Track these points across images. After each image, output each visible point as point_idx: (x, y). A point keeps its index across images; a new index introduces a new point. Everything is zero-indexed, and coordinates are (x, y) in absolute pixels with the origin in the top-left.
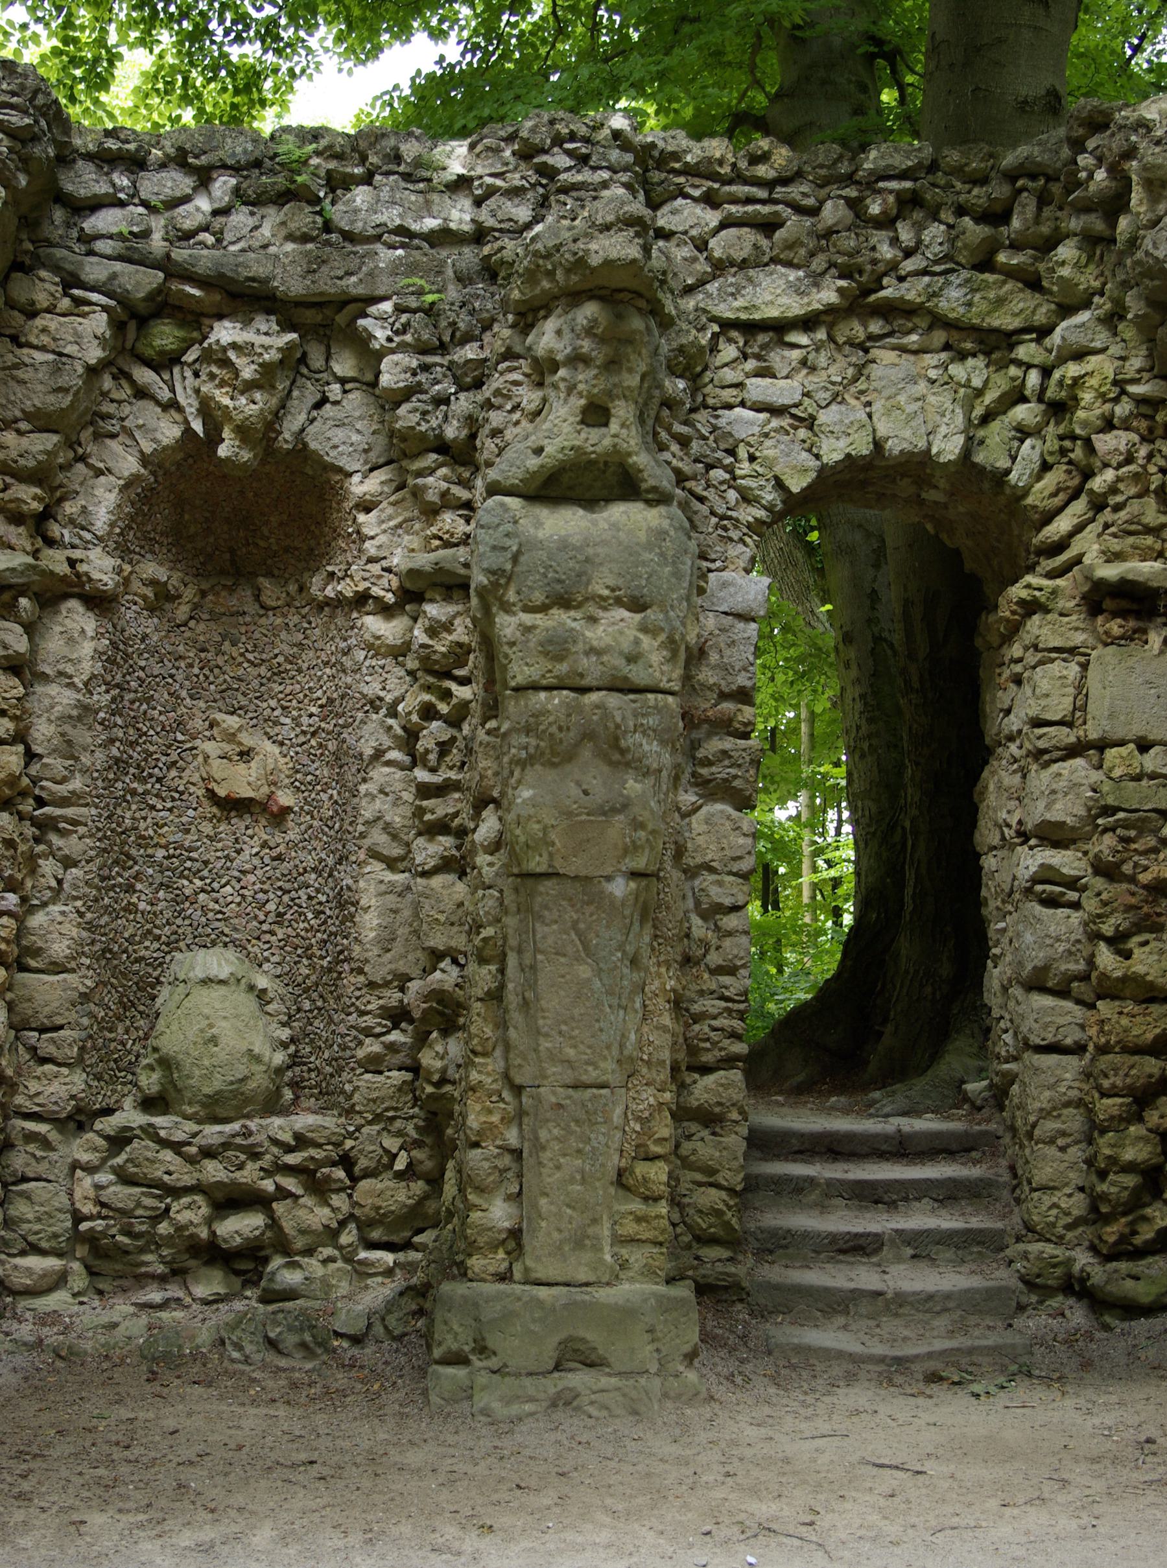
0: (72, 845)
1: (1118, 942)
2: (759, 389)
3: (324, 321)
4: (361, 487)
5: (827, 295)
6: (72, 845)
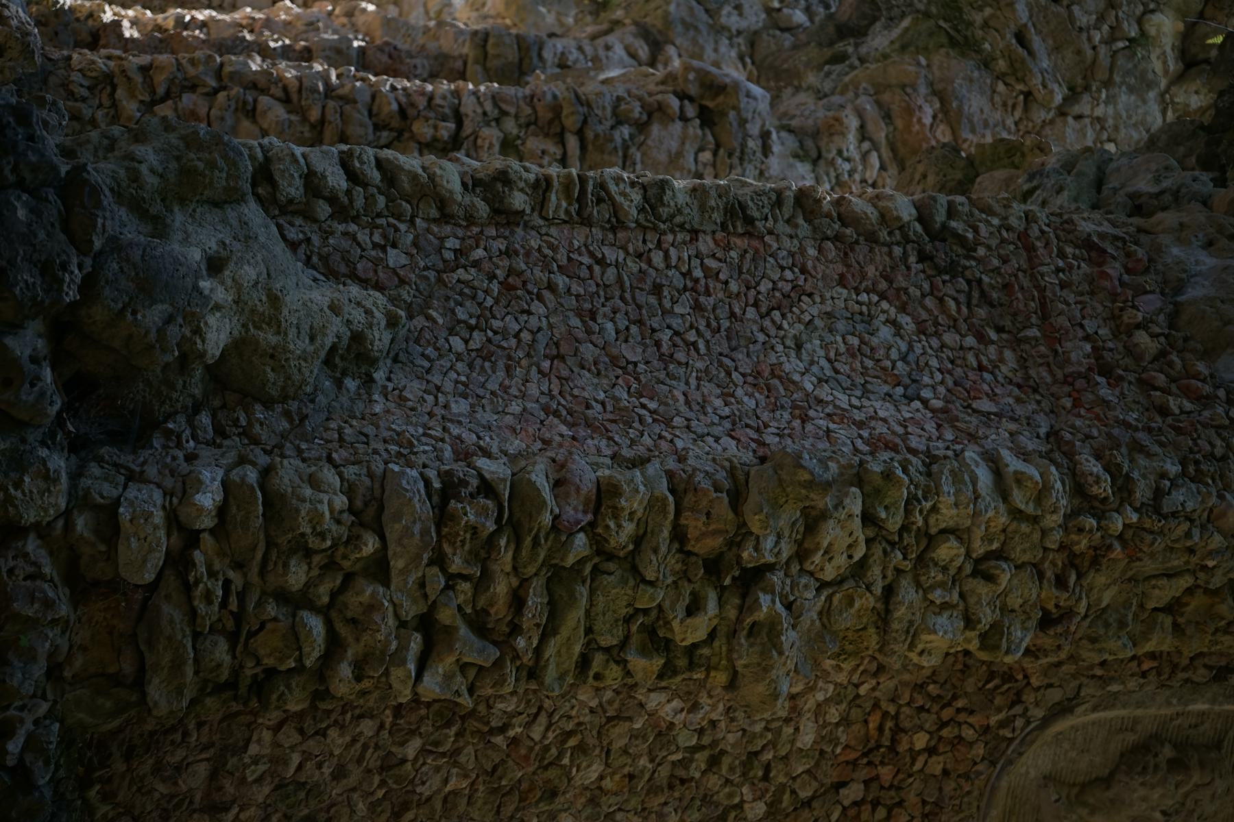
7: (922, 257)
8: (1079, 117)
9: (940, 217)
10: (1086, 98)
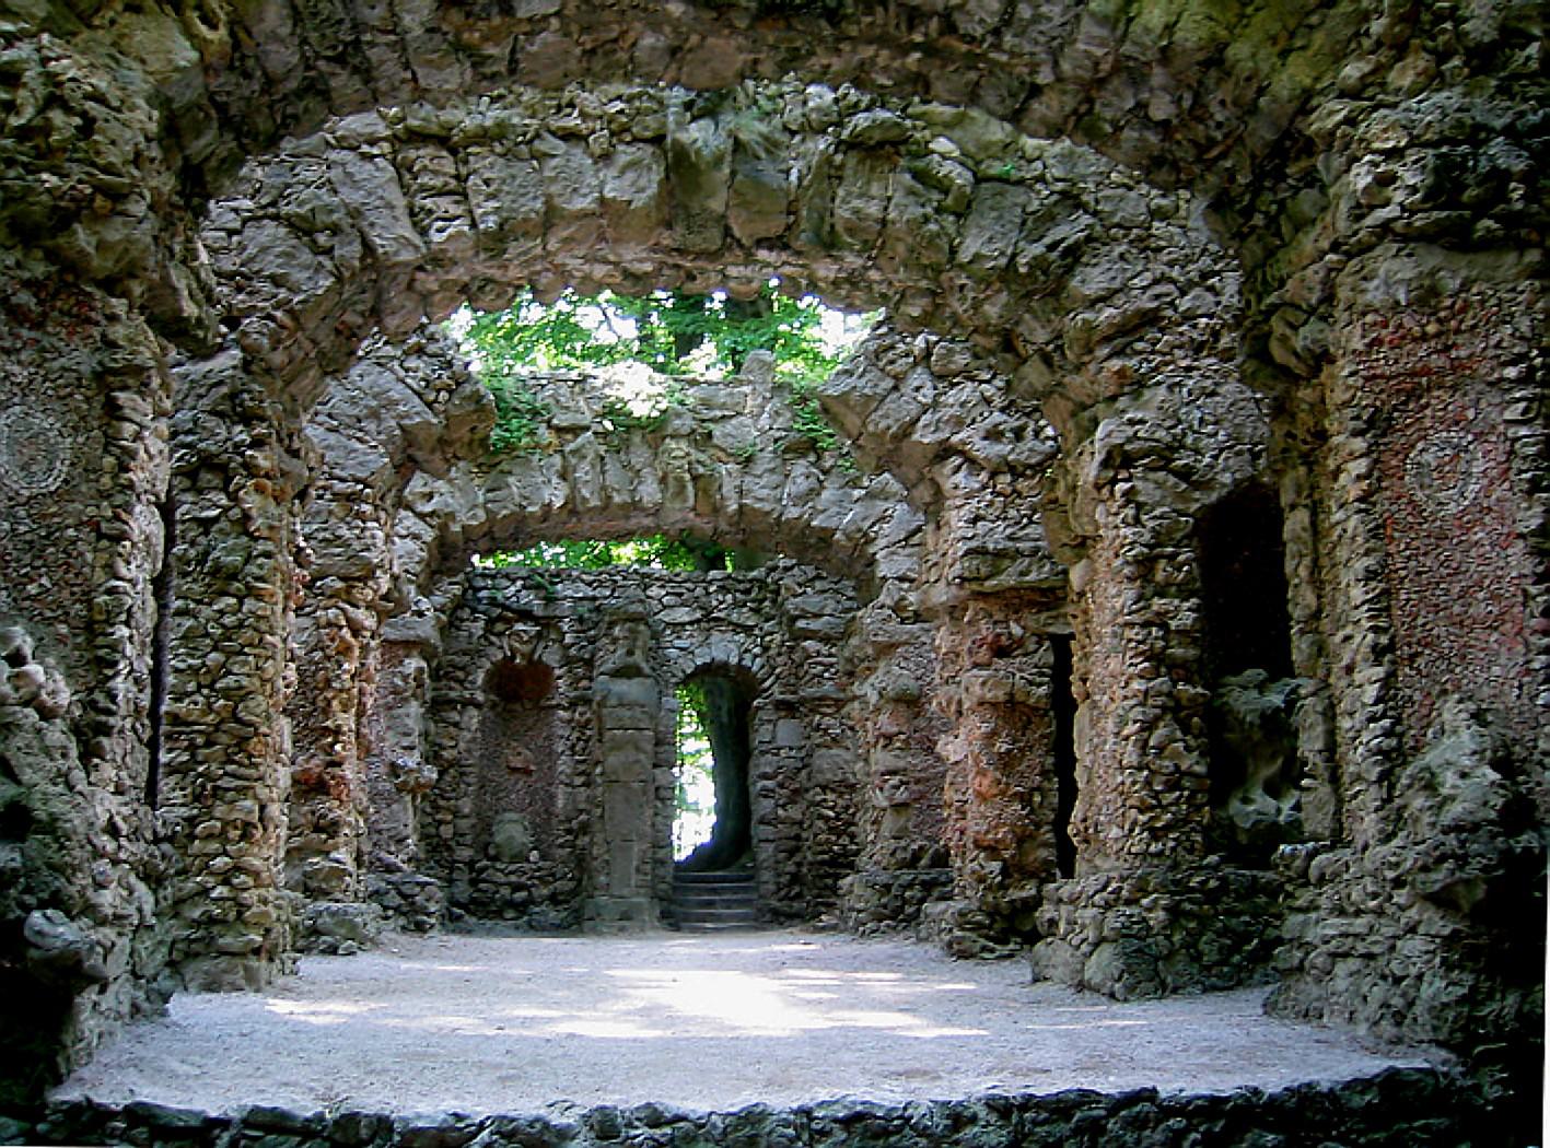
0: (471, 779)
1: (783, 806)
2: (677, 643)
3: (548, 624)
4: (558, 672)
5: (698, 615)
6: (471, 779)
7: (1384, 435)
8: (1097, 202)
9: (1360, 425)
10: (1085, 198)
